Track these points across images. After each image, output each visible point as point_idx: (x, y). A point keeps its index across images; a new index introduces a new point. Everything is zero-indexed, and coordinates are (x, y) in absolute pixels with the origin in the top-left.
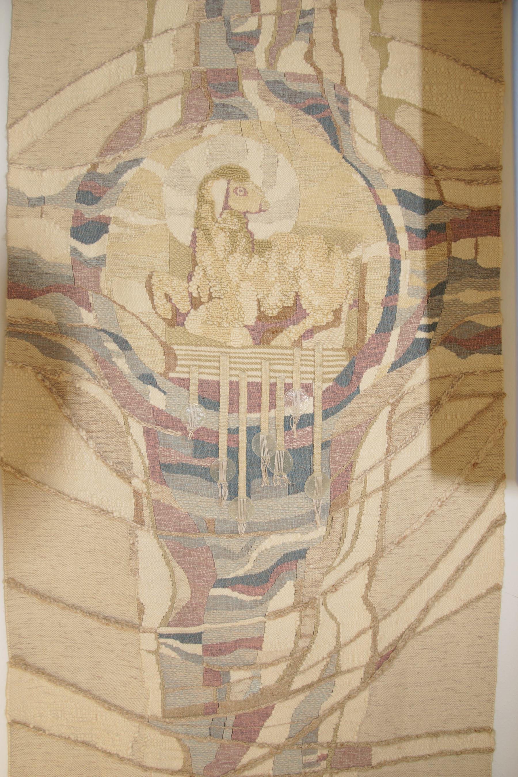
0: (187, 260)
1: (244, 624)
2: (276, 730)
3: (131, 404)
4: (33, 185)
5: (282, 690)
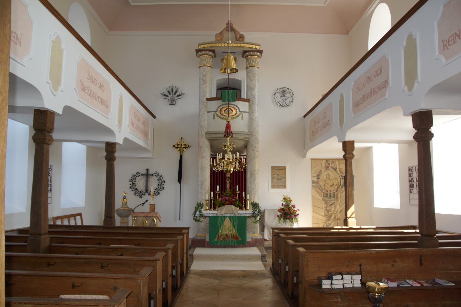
0: (325, 181)
1: (330, 208)
2: (333, 217)
3: (322, 191)
4: (313, 175)
5: (333, 214)
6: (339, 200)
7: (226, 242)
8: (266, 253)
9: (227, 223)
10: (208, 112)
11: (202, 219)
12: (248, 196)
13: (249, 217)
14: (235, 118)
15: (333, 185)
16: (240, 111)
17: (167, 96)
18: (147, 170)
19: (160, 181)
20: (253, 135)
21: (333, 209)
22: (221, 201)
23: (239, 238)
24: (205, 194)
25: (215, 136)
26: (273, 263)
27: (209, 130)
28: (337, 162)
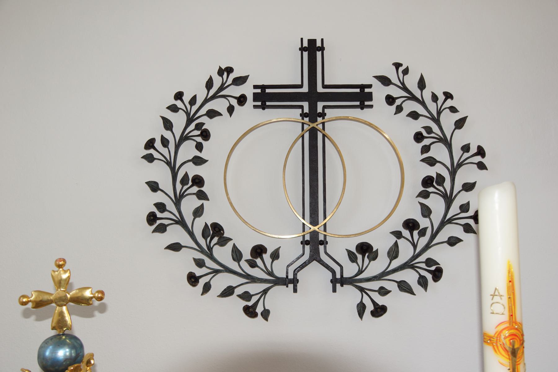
18: (312, 49)
19: (439, 152)
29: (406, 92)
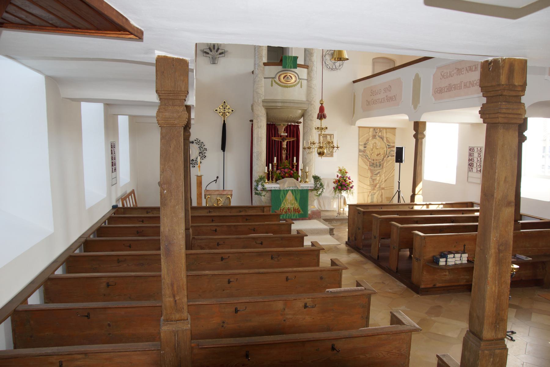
0: (372, 150)
2: (378, 186)
3: (368, 161)
6: (384, 170)
7: (288, 215)
8: (332, 227)
9: (290, 197)
10: (265, 78)
11: (264, 193)
12: (307, 168)
13: (312, 190)
14: (295, 86)
15: (380, 154)
16: (299, 78)
17: (208, 53)
20: (312, 104)
21: (378, 178)
22: (280, 174)
23: (301, 211)
24: (261, 167)
25: (273, 104)
26: (349, 238)
27: (266, 98)
28: (384, 131)
29: (198, 142)
